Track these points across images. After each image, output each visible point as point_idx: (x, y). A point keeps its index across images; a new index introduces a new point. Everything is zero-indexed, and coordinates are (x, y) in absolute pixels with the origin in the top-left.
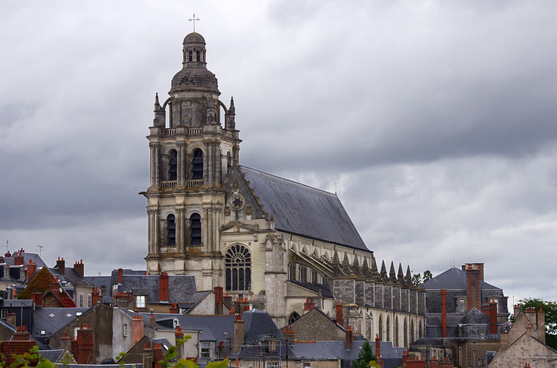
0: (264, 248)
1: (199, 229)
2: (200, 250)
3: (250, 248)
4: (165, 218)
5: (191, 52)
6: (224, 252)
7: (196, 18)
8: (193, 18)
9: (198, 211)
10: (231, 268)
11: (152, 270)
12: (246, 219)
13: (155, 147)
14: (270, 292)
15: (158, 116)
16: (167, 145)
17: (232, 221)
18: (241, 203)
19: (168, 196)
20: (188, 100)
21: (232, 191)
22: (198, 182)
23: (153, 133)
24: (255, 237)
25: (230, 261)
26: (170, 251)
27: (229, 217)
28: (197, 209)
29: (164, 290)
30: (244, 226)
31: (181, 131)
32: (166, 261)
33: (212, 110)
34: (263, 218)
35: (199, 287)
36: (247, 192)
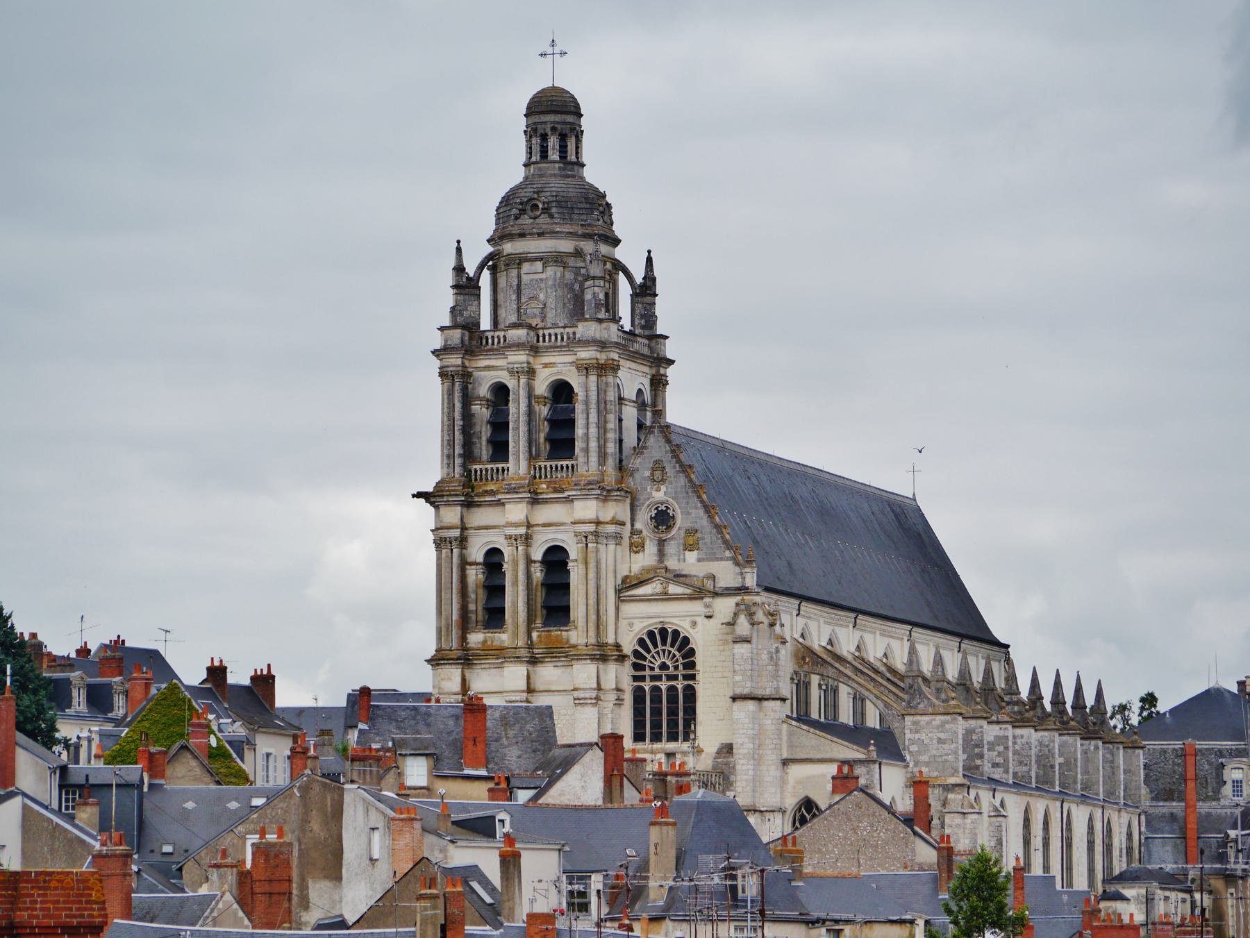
1: (567, 587)
2: (568, 641)
4: (480, 559)
5: (544, 137)
6: (629, 646)
7: (557, 50)
8: (549, 51)
9: (563, 541)
10: (647, 686)
11: (446, 690)
13: (453, 376)
15: (461, 298)
16: (483, 373)
19: (486, 501)
20: (536, 259)
21: (649, 490)
22: (562, 466)
23: (449, 343)
24: (707, 606)
25: (642, 668)
27: (641, 554)
28: (559, 536)
29: (475, 741)
30: (678, 577)
31: (519, 338)
33: (597, 284)
34: (728, 559)
36: (687, 493)
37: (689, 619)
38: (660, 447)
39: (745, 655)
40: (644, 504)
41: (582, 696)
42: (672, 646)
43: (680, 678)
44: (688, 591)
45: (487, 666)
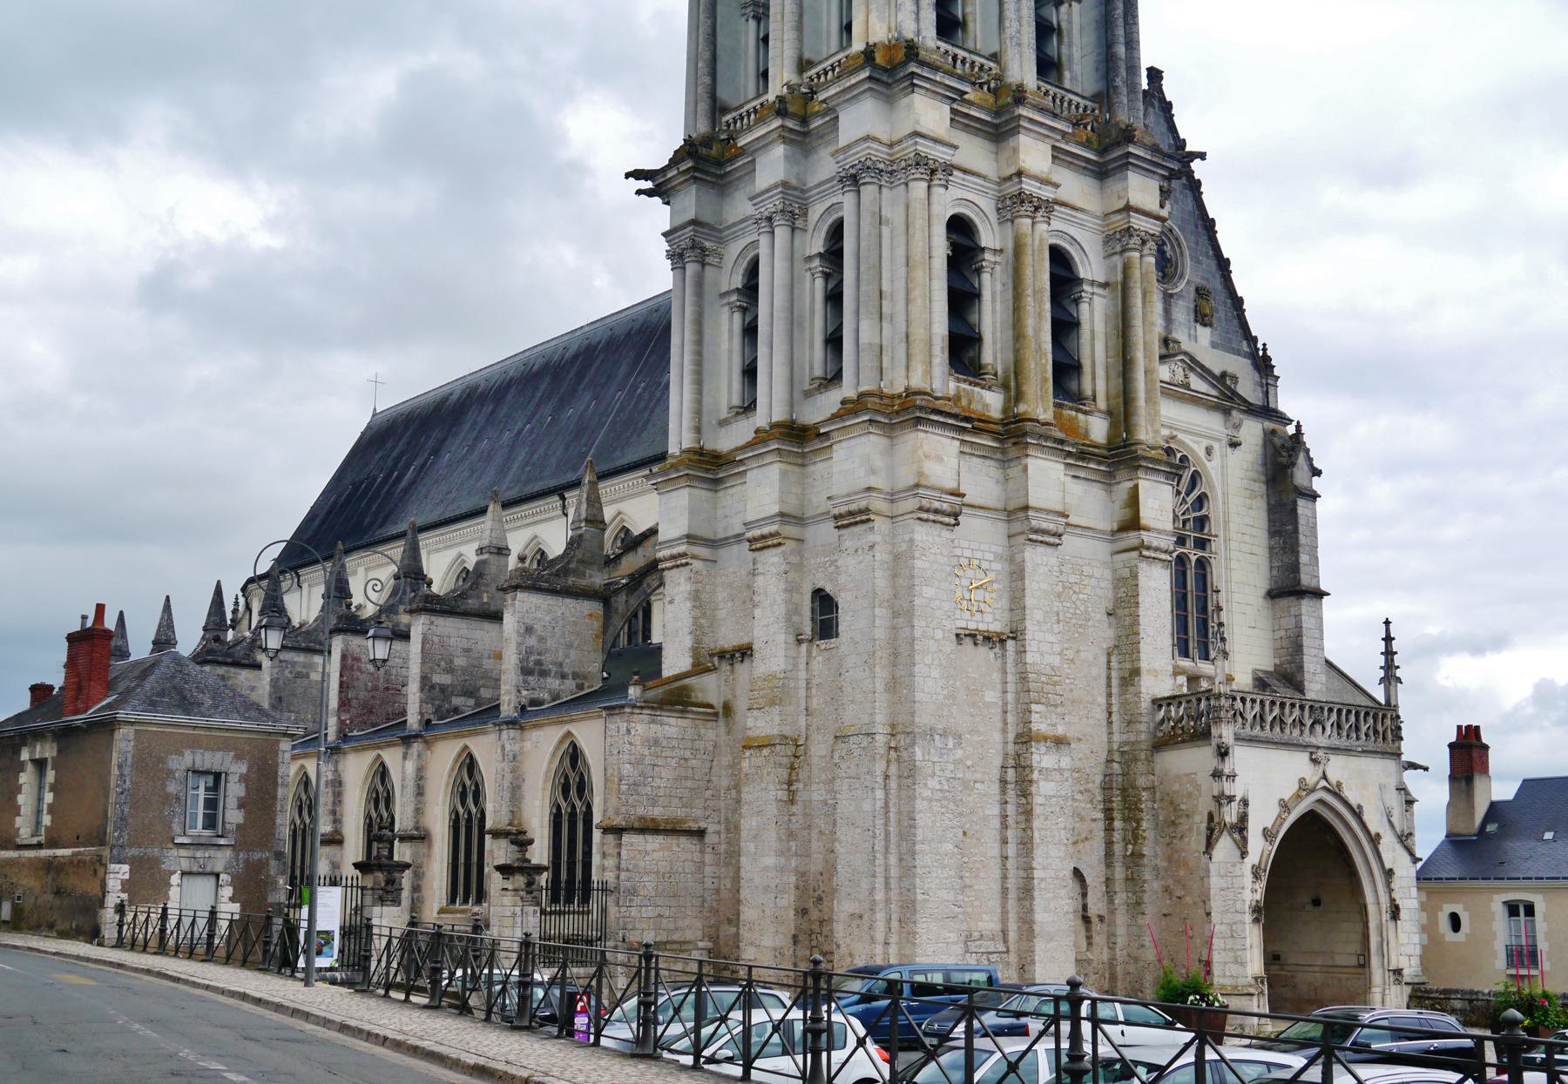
0: (1257, 484)
3: (1213, 473)
11: (933, 481)
12: (1196, 341)
18: (1169, 265)
19: (967, 116)
26: (970, 402)
28: (1072, 231)
36: (1196, 227)
38: (1162, 134)
41: (1155, 544)
43: (1190, 543)
44: (1214, 392)
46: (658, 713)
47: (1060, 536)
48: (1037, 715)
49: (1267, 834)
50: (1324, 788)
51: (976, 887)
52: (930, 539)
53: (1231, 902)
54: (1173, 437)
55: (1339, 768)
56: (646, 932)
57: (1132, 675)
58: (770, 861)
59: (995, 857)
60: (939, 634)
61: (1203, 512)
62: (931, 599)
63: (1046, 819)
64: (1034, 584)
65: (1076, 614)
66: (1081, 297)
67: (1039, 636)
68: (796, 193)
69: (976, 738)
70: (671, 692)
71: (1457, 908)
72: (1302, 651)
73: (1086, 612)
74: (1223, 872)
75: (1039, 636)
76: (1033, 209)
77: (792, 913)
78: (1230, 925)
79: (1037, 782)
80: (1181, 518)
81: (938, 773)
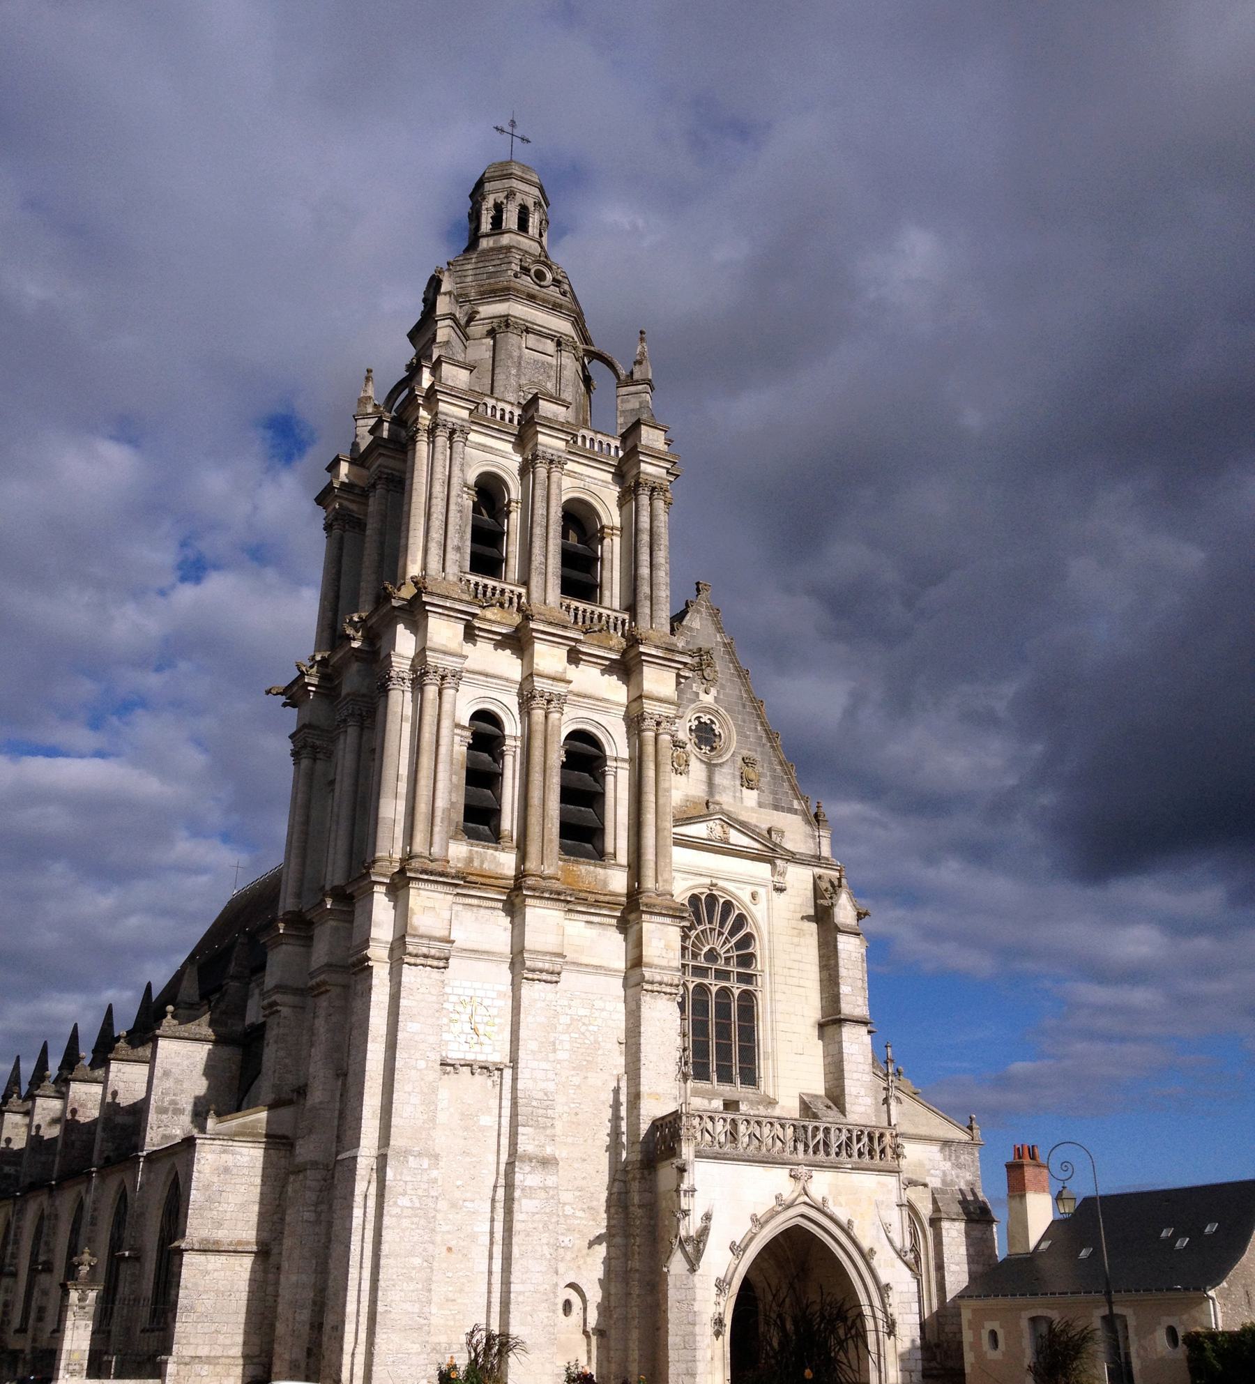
1: (601, 796)
2: (605, 883)
4: (466, 722)
11: (422, 930)
12: (742, 803)
14: (860, 1100)
17: (694, 797)
18: (717, 740)
20: (547, 336)
21: (694, 689)
26: (482, 862)
28: (597, 717)
31: (557, 416)
32: (463, 904)
34: (795, 812)
35: (599, 1044)
36: (744, 706)
37: (750, 889)
39: (854, 954)
40: (689, 706)
41: (658, 978)
42: (710, 922)
43: (733, 977)
45: (475, 901)
46: (230, 1143)
47: (559, 974)
48: (524, 1137)
49: (737, 1249)
50: (805, 1203)
51: (459, 1301)
52: (419, 980)
53: (683, 1314)
54: (712, 885)
55: (822, 1184)
56: (200, 1348)
57: (635, 1098)
58: (294, 1278)
59: (482, 1273)
60: (422, 1064)
61: (750, 950)
62: (415, 1033)
63: (528, 1235)
64: (530, 1019)
65: (585, 1043)
66: (605, 771)
67: (534, 1064)
68: (365, 699)
69: (468, 1159)
70: (244, 1125)
71: (995, 1325)
72: (843, 1075)
73: (596, 1042)
74: (678, 1284)
75: (534, 1064)
76: (545, 702)
77: (307, 1327)
78: (684, 1337)
79: (519, 1200)
80: (723, 956)
81: (409, 1192)
